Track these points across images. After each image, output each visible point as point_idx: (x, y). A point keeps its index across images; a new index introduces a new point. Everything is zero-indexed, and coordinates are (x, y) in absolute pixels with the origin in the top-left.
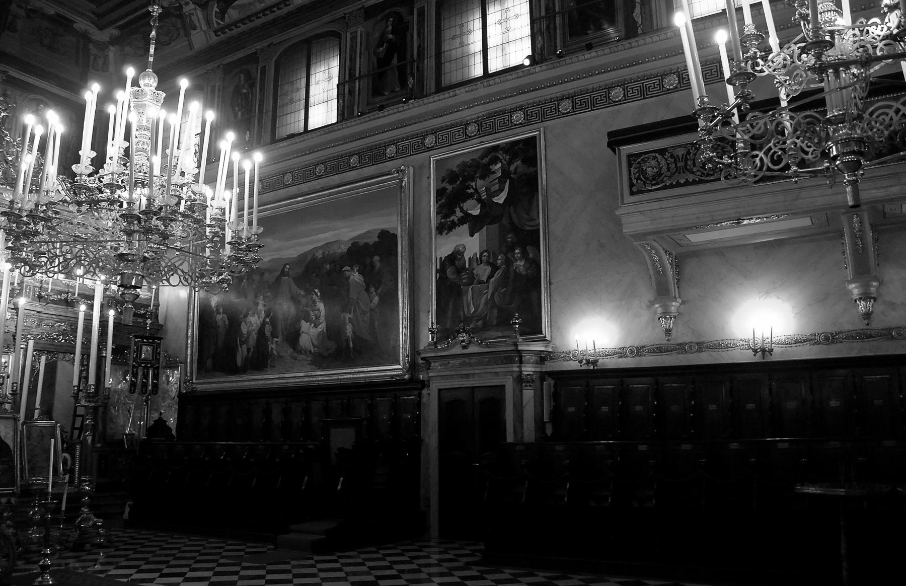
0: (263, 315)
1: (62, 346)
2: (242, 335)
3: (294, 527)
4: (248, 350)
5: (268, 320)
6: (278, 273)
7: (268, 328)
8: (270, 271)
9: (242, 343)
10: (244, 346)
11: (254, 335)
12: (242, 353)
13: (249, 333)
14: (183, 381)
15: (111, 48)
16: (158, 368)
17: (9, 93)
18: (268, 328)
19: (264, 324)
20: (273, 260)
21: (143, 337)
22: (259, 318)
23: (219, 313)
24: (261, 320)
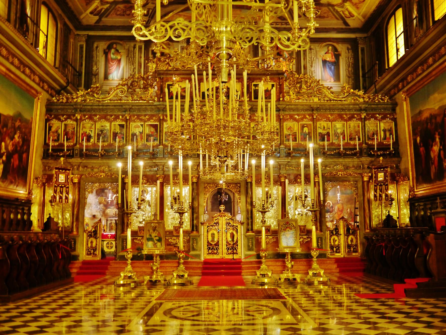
0: (439, 145)
1: (340, 178)
2: (431, 158)
3: (406, 280)
4: (435, 168)
5: (441, 148)
6: (442, 116)
7: (442, 152)
8: (439, 115)
9: (433, 164)
10: (433, 166)
11: (437, 158)
12: (433, 170)
13: (434, 157)
14: (412, 190)
15: (346, 4)
16: (387, 185)
17: (312, 47)
18: (442, 152)
19: (440, 150)
20: (440, 108)
21: (377, 168)
22: (438, 146)
23: (421, 147)
24: (439, 147)
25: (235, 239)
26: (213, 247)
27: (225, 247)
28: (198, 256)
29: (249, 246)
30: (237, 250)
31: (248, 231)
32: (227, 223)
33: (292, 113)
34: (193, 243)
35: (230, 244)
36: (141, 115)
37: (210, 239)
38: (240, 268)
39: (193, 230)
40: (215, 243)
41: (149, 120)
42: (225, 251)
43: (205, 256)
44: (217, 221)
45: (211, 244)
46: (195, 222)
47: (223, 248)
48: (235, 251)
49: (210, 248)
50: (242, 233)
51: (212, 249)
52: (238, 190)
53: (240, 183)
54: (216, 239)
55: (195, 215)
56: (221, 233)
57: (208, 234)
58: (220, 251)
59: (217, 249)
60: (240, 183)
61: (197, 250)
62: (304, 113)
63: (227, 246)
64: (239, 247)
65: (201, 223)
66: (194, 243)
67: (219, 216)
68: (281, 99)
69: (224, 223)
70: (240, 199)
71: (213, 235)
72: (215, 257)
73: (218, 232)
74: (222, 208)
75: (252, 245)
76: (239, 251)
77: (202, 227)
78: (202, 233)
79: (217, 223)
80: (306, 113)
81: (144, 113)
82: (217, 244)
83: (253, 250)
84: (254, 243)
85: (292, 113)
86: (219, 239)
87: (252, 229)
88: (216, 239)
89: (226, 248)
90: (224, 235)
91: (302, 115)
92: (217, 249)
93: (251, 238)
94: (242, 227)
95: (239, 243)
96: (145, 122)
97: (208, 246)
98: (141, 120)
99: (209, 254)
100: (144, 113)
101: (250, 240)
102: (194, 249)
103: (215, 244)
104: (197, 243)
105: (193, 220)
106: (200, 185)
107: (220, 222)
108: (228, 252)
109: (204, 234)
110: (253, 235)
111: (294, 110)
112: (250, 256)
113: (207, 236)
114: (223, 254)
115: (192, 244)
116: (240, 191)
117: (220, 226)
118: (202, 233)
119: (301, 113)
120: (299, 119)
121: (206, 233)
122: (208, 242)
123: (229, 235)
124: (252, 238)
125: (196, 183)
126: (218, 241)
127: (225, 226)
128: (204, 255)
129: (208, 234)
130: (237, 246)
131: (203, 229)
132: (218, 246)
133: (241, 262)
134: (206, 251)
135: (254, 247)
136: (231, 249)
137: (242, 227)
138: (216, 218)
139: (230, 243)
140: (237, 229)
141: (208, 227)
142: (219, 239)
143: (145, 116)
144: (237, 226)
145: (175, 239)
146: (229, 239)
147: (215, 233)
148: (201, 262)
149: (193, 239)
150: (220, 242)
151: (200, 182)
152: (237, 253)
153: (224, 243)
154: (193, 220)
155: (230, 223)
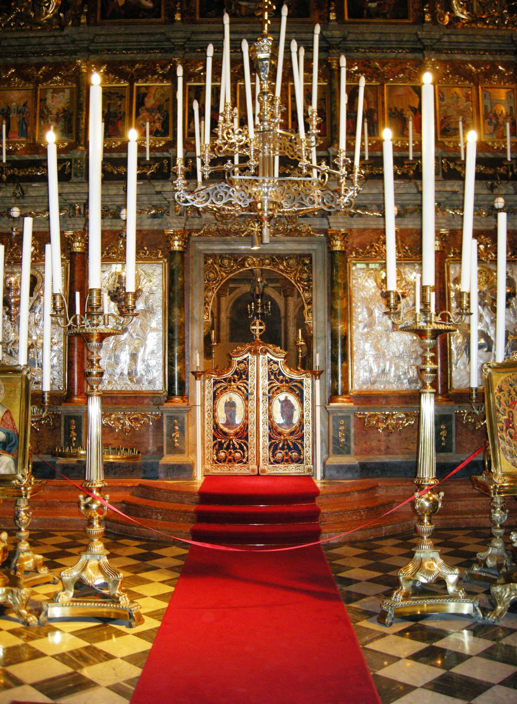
25: (296, 420)
26: (229, 442)
27: (264, 441)
28: (185, 470)
29: (336, 440)
30: (299, 453)
31: (333, 395)
32: (271, 372)
33: (458, 57)
34: (172, 430)
35: (280, 434)
36: (29, 66)
37: (222, 417)
38: (314, 515)
39: (171, 393)
40: (238, 429)
41: (48, 77)
42: (264, 453)
43: (208, 467)
44: (242, 365)
45: (225, 434)
46: (177, 368)
47: (260, 443)
48: (295, 454)
49: (221, 445)
50: (318, 402)
51: (228, 448)
52: (305, 276)
53: (309, 256)
54: (238, 420)
55: (177, 349)
56: (252, 404)
57: (214, 404)
58: (251, 453)
59: (241, 448)
60: (309, 256)
61: (181, 452)
62: (491, 59)
63: (270, 438)
64: (307, 441)
65: (193, 373)
66: (174, 431)
67: (249, 351)
68: (427, 18)
69: (263, 371)
70: (310, 303)
71: (230, 406)
72: (237, 469)
73: (247, 399)
74: (257, 327)
75: (347, 438)
76: (307, 452)
77: (198, 383)
78: (198, 402)
79: (242, 374)
80: (498, 58)
81: (34, 60)
82: (243, 434)
83: (348, 452)
84: (352, 430)
85: (458, 57)
86: (247, 418)
87: (345, 392)
88: (238, 420)
89: (268, 444)
90: (263, 407)
91: (485, 63)
92: (241, 448)
93: (343, 418)
94: (318, 382)
95: (308, 428)
96: (38, 82)
97: (215, 438)
98: (27, 78)
99: (219, 460)
100: (34, 60)
101: (342, 422)
102: (174, 450)
103: (236, 434)
104: (182, 430)
105: (171, 364)
106: (191, 261)
107: (252, 369)
108: (274, 455)
109: (203, 405)
110: (350, 410)
111: (463, 52)
112: (339, 468)
113: (215, 411)
114: (259, 461)
115: (169, 435)
116: (309, 280)
117: (252, 382)
118: (198, 402)
119: (484, 58)
120: (478, 74)
121: (208, 404)
122: (216, 427)
123: (277, 407)
124: (347, 418)
125: (179, 252)
126: (245, 426)
127: (264, 382)
128: (203, 463)
129: (214, 404)
130: (302, 438)
131: (199, 390)
132: (247, 438)
133: (316, 493)
134: (210, 453)
135: (352, 444)
136: (283, 449)
137: (318, 382)
138: (240, 359)
139: (280, 429)
140: (302, 391)
141: (216, 382)
142: (247, 418)
143: (38, 66)
144: (301, 382)
145: (119, 419)
146: (279, 419)
147: (237, 399)
148: (190, 494)
149: (171, 418)
150: (252, 428)
151: (191, 252)
152: (300, 461)
153: (264, 429)
154: (171, 364)
155: (280, 373)
